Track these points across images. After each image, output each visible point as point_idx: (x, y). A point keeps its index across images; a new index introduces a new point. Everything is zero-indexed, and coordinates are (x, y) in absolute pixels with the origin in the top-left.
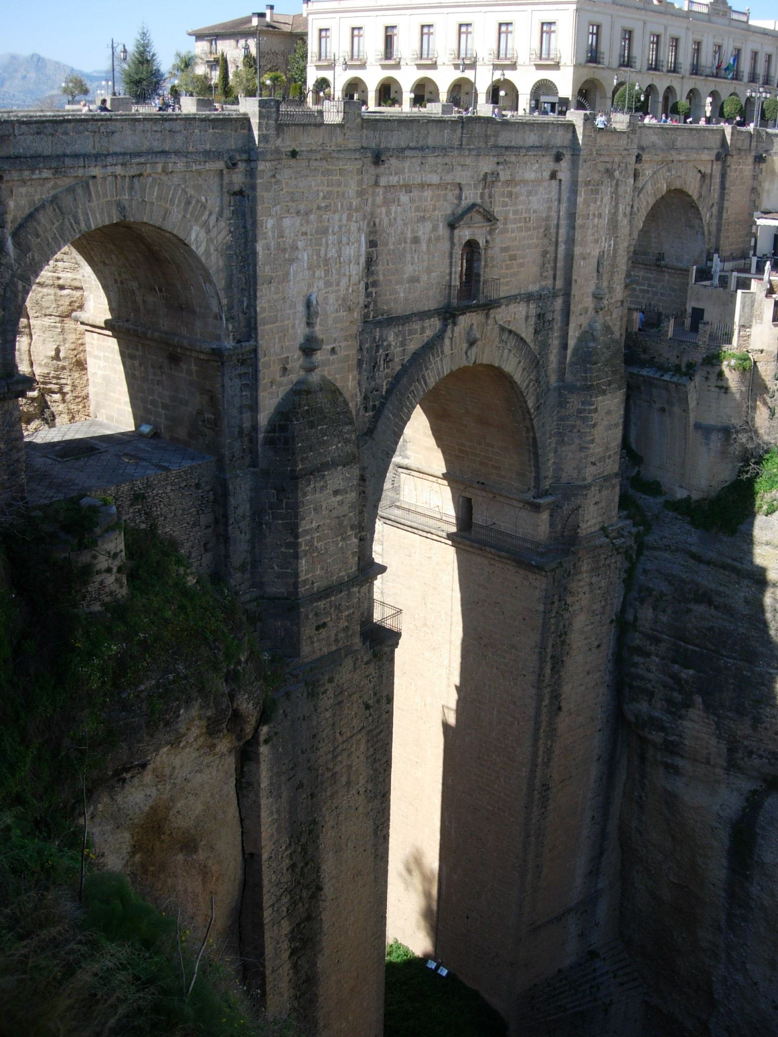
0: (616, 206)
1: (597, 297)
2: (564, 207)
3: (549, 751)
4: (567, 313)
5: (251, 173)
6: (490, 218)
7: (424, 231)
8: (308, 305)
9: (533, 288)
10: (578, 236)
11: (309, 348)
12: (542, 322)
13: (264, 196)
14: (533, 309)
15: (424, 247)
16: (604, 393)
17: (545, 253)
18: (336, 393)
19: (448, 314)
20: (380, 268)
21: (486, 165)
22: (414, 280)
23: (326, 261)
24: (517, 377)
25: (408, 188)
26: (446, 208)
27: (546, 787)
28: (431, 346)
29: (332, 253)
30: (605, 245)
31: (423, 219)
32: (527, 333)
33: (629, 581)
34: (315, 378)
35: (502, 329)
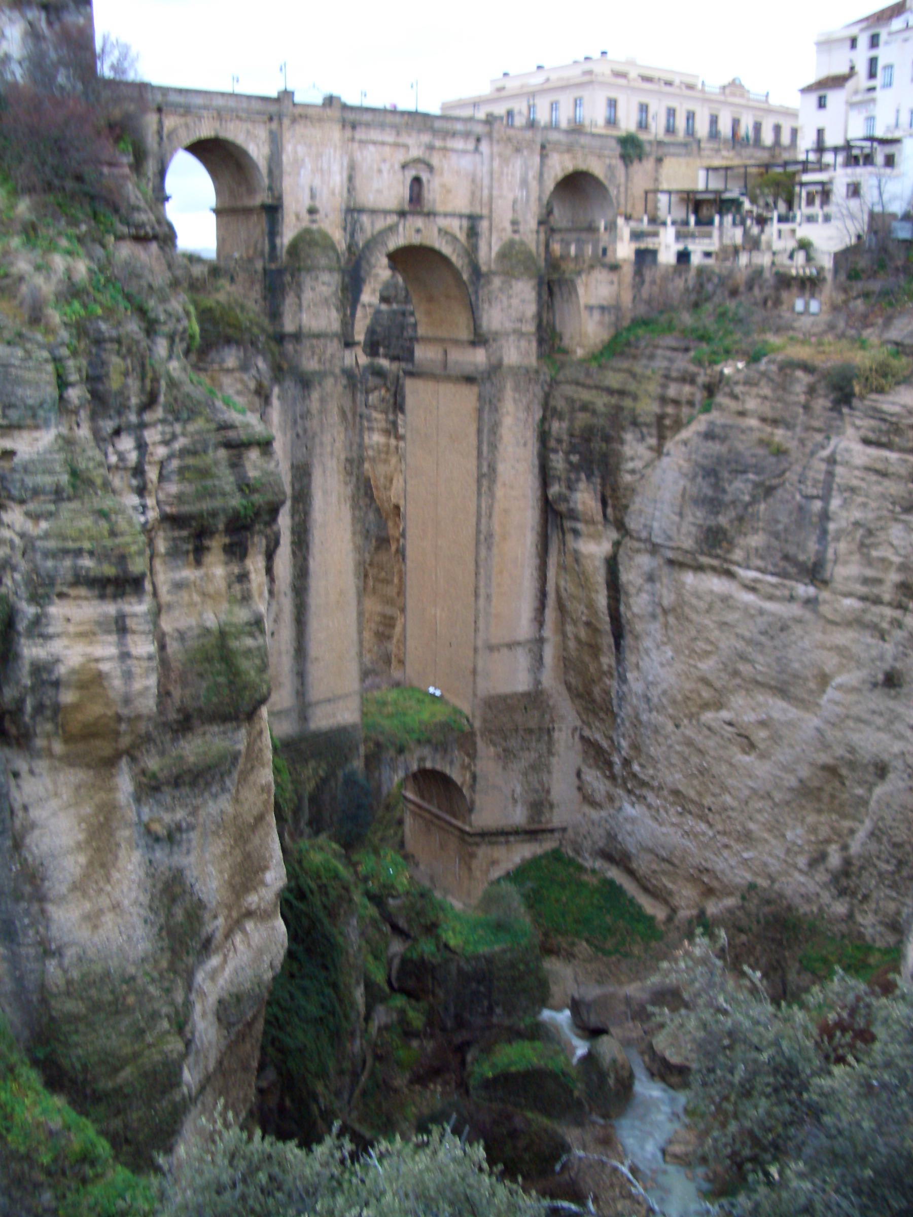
0: (527, 174)
1: (514, 223)
2: (486, 169)
3: (491, 508)
4: (490, 230)
5: (281, 124)
6: (430, 168)
7: (385, 167)
8: (311, 190)
9: (466, 210)
10: (495, 185)
11: (312, 211)
12: (473, 233)
13: (287, 135)
14: (465, 223)
15: (385, 174)
16: (517, 279)
17: (473, 193)
18: (325, 236)
19: (402, 214)
20: (358, 182)
21: (426, 138)
22: (379, 191)
23: (322, 170)
24: (454, 259)
25: (374, 143)
26: (401, 157)
27: (490, 535)
28: (392, 229)
29: (325, 166)
30: (520, 194)
31: (384, 161)
32: (462, 237)
33: (546, 406)
34: (315, 227)
35: (440, 230)
